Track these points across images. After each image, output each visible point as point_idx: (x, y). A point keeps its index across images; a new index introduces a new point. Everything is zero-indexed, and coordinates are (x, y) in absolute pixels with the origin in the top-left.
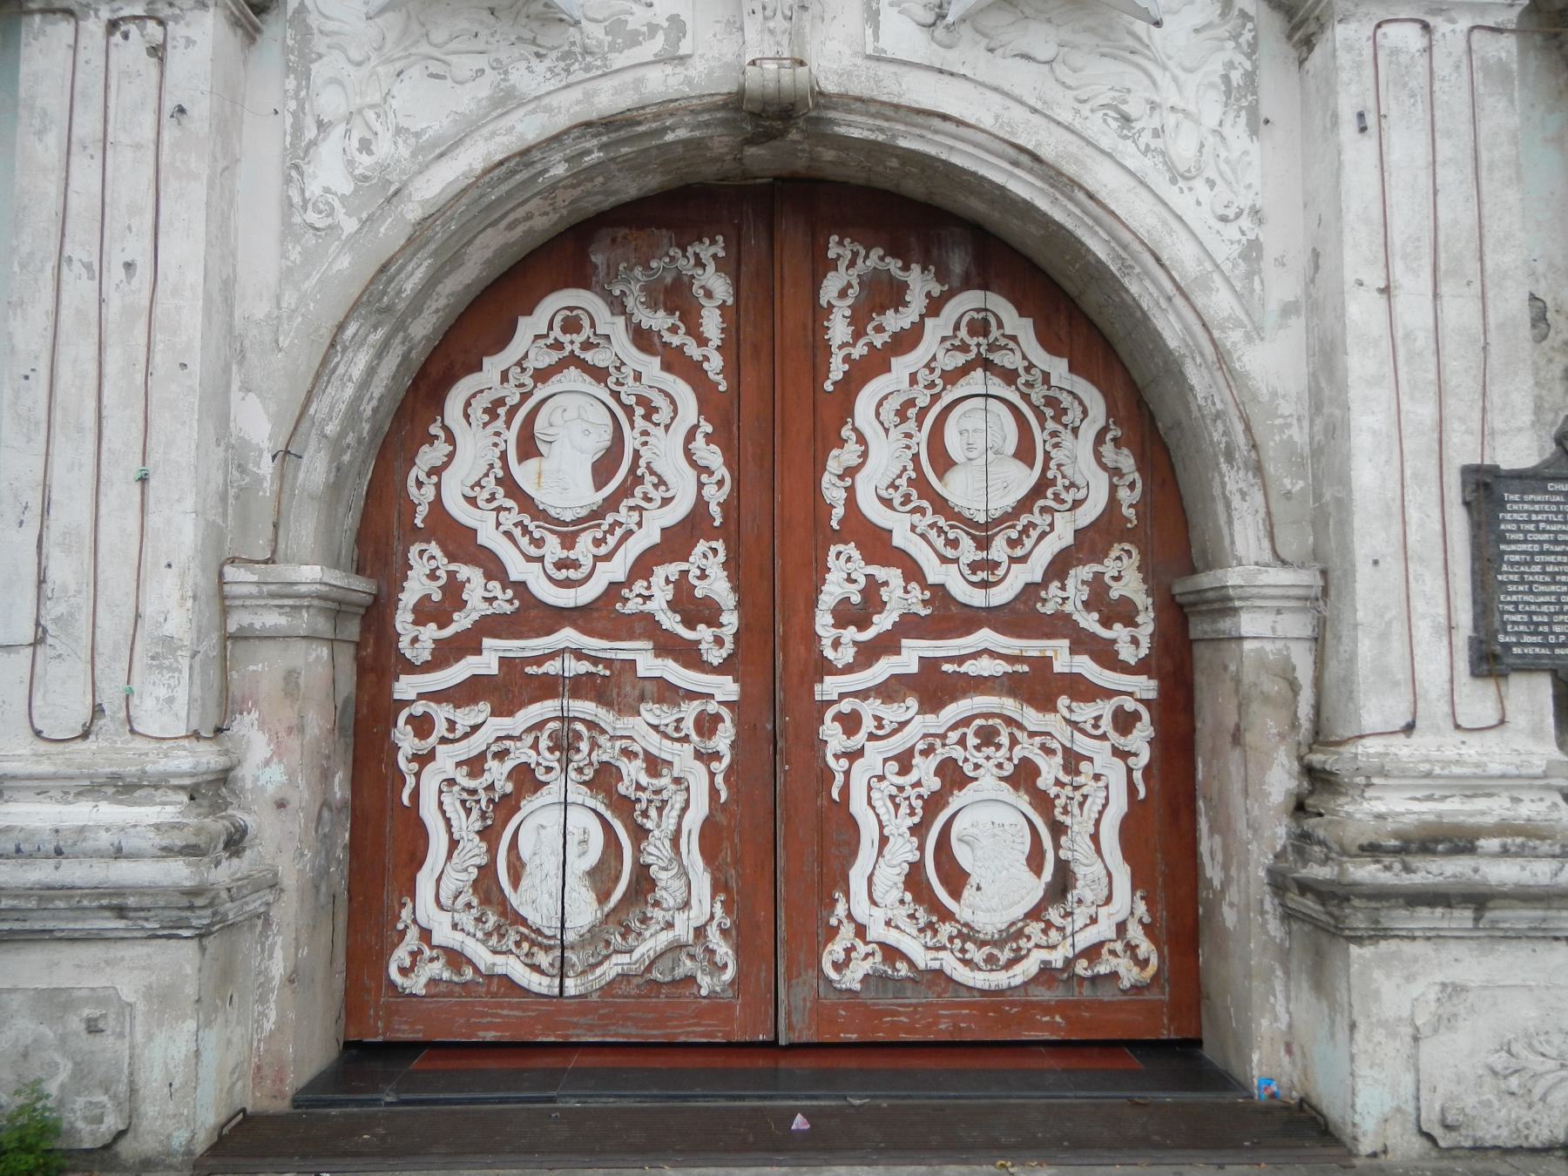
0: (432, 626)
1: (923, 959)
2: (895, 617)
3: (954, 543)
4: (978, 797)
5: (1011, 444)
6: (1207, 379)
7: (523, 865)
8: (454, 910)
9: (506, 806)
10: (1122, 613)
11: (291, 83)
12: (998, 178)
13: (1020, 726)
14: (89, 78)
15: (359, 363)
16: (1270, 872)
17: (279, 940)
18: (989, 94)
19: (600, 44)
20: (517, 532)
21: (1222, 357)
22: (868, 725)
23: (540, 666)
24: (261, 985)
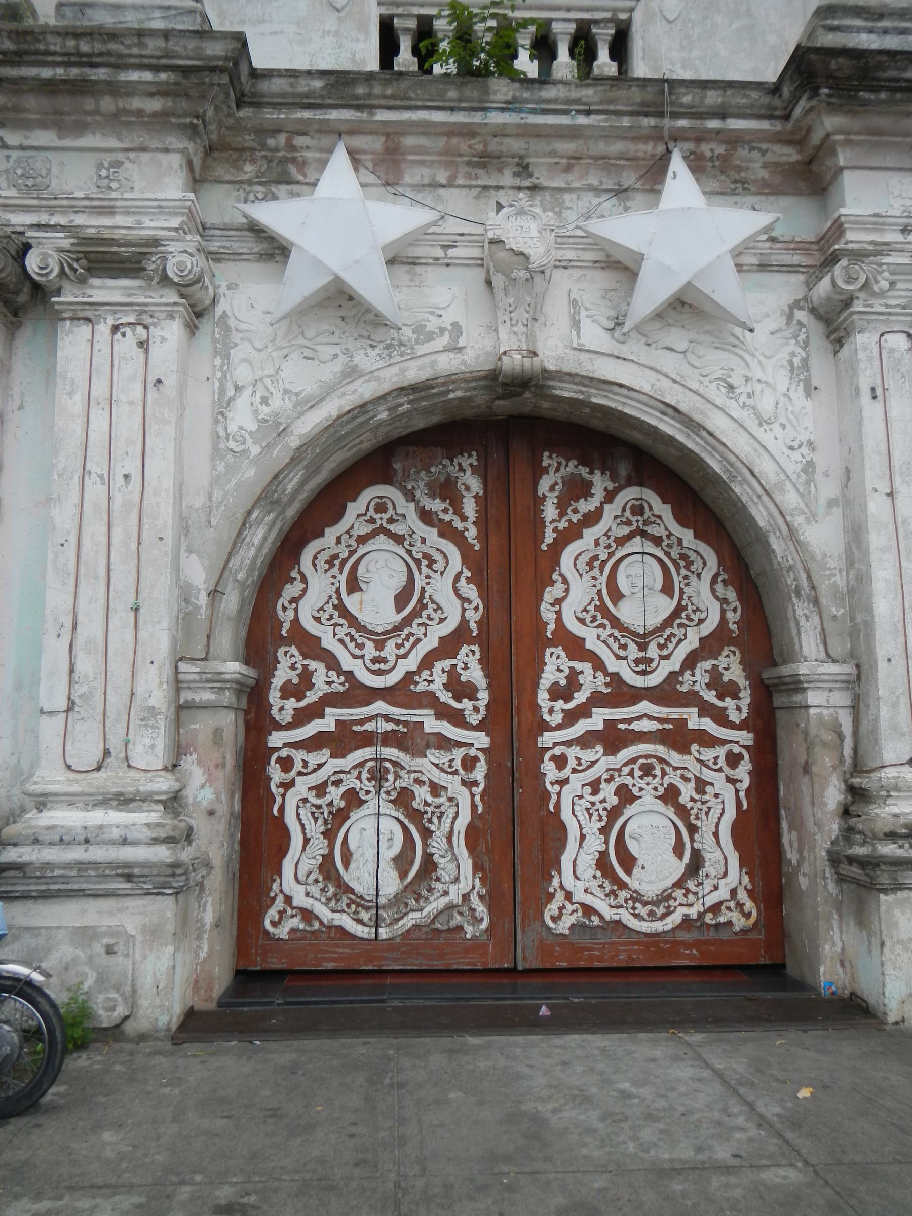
0: (293, 700)
1: (609, 914)
2: (588, 694)
3: (624, 647)
4: (642, 809)
5: (659, 585)
6: (784, 546)
7: (351, 854)
8: (307, 884)
9: (340, 816)
10: (729, 690)
11: (218, 361)
12: (653, 422)
13: (668, 764)
14: (102, 360)
16: (829, 852)
17: (210, 900)
18: (648, 372)
19: (410, 340)
20: (347, 640)
21: (792, 532)
22: (572, 763)
23: (362, 725)
24: (198, 929)
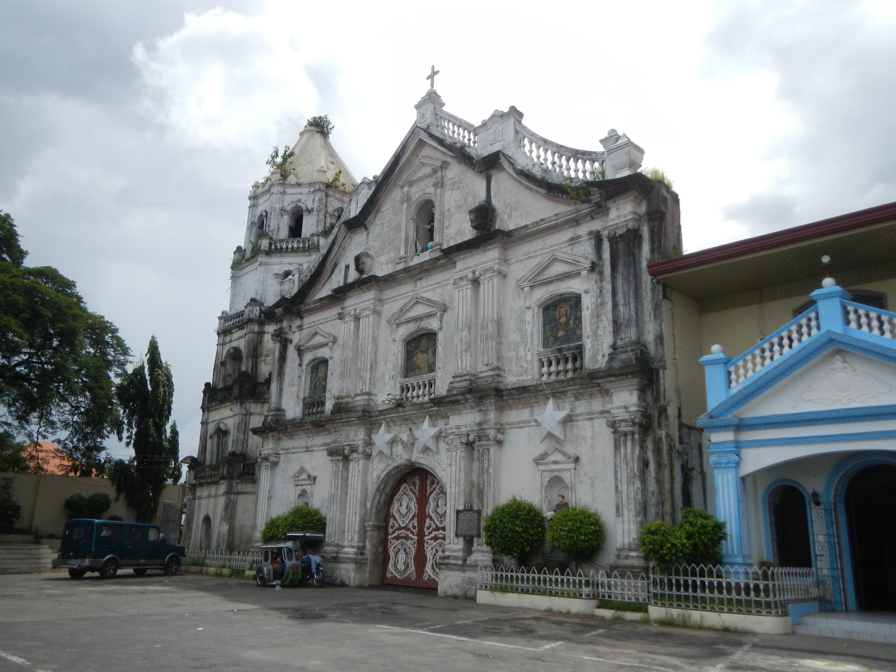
9: (397, 553)
15: (378, 497)
